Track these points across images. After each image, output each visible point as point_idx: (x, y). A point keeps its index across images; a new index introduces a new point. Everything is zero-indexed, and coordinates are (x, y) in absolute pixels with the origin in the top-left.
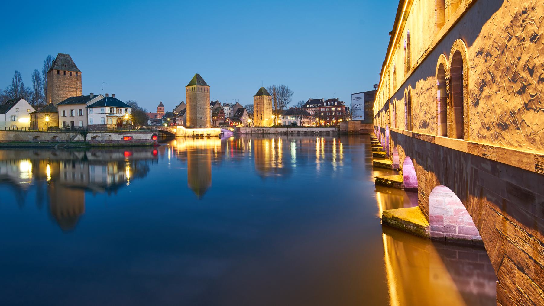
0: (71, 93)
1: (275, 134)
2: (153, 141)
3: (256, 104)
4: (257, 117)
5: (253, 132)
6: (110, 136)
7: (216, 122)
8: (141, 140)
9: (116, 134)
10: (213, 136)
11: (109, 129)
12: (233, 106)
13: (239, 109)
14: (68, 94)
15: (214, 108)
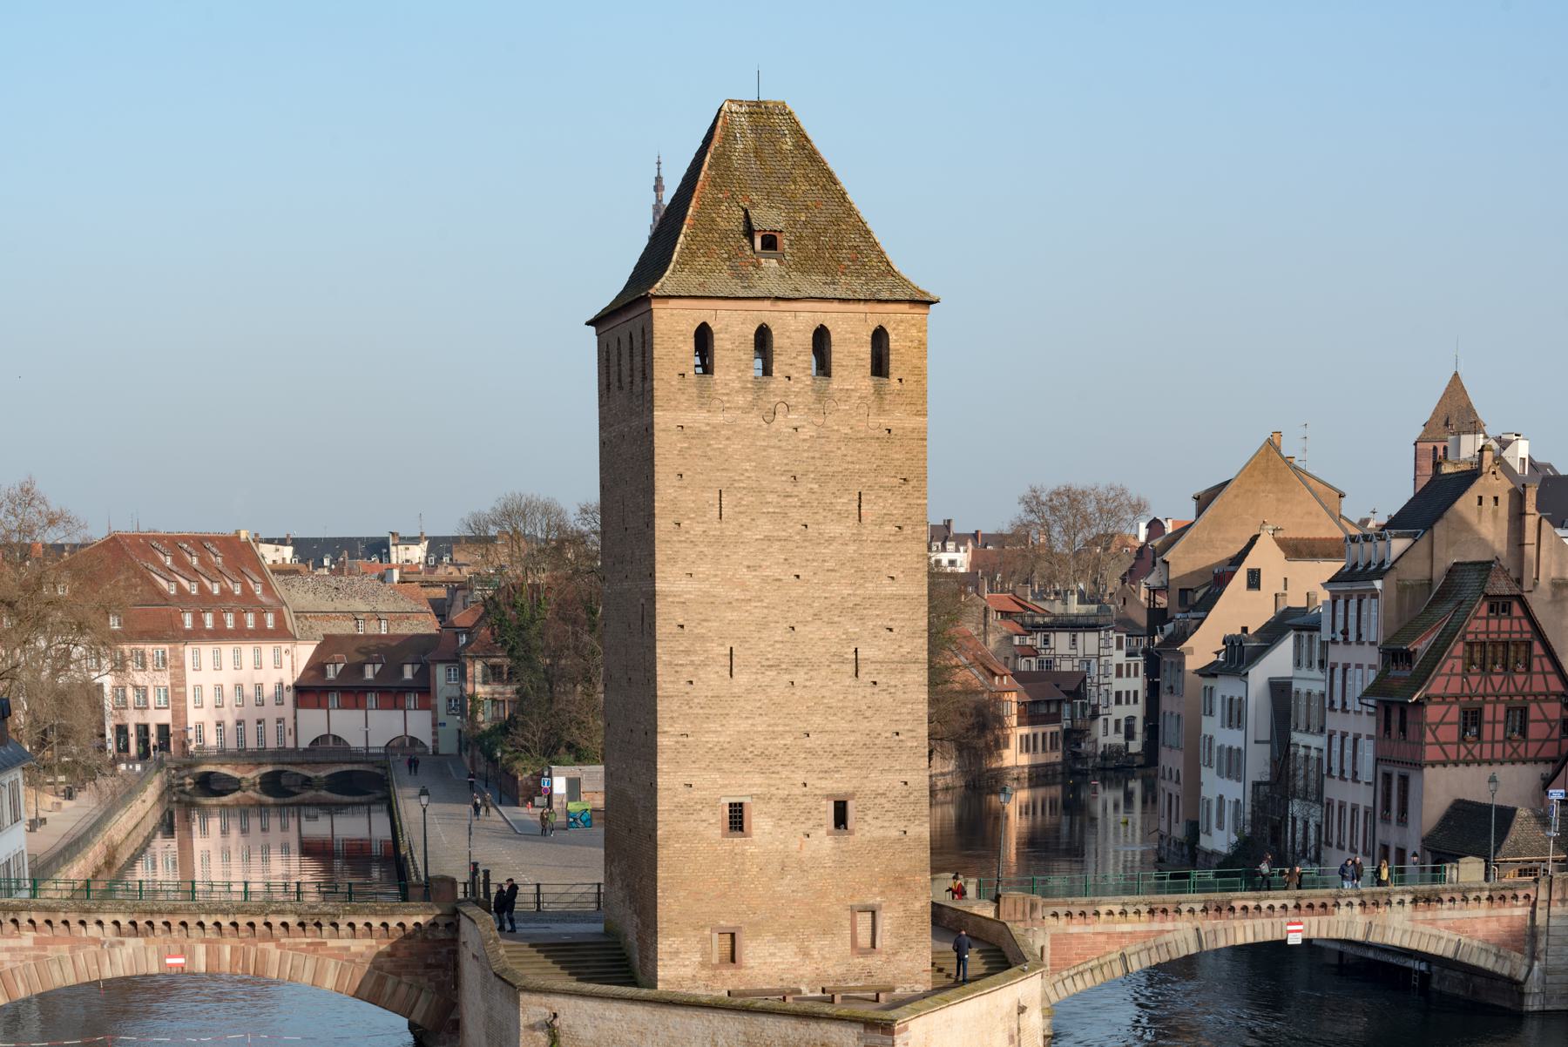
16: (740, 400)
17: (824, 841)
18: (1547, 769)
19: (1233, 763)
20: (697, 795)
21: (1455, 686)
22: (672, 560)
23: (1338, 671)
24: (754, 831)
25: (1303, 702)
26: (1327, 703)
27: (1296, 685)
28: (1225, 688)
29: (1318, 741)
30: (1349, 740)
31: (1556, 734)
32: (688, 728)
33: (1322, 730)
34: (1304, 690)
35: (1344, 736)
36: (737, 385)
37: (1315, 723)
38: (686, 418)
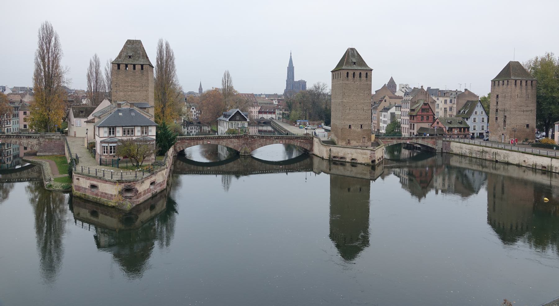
0: (134, 94)
1: (522, 166)
2: (123, 199)
3: (496, 96)
4: (496, 122)
5: (474, 155)
6: (78, 179)
7: (414, 125)
8: (106, 194)
9: (84, 178)
10: (361, 164)
11: (104, 162)
12: (459, 95)
13: (468, 101)
14: (130, 96)
15: (414, 101)
16: (352, 80)
17: (359, 130)
18: (431, 124)
19: (385, 122)
20: (346, 124)
21: (420, 114)
22: (344, 98)
23: (403, 112)
24: (352, 129)
25: (397, 115)
26: (401, 115)
27: (395, 113)
28: (383, 113)
29: (400, 120)
30: (405, 120)
31: (432, 119)
32: (345, 116)
33: (400, 118)
34: (397, 114)
35: (404, 119)
36: (351, 79)
37: (399, 118)
38: (345, 82)
